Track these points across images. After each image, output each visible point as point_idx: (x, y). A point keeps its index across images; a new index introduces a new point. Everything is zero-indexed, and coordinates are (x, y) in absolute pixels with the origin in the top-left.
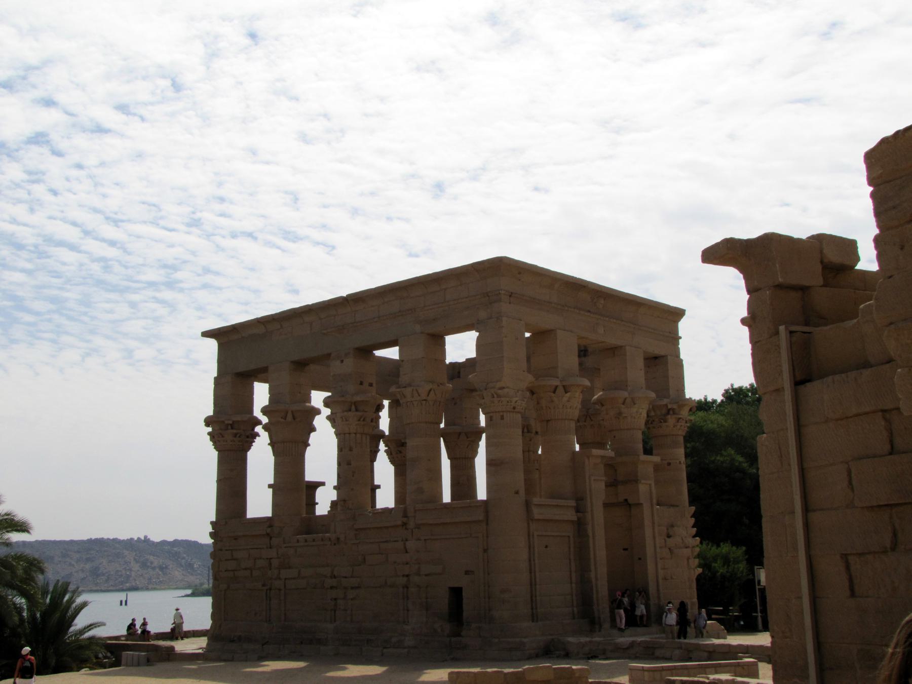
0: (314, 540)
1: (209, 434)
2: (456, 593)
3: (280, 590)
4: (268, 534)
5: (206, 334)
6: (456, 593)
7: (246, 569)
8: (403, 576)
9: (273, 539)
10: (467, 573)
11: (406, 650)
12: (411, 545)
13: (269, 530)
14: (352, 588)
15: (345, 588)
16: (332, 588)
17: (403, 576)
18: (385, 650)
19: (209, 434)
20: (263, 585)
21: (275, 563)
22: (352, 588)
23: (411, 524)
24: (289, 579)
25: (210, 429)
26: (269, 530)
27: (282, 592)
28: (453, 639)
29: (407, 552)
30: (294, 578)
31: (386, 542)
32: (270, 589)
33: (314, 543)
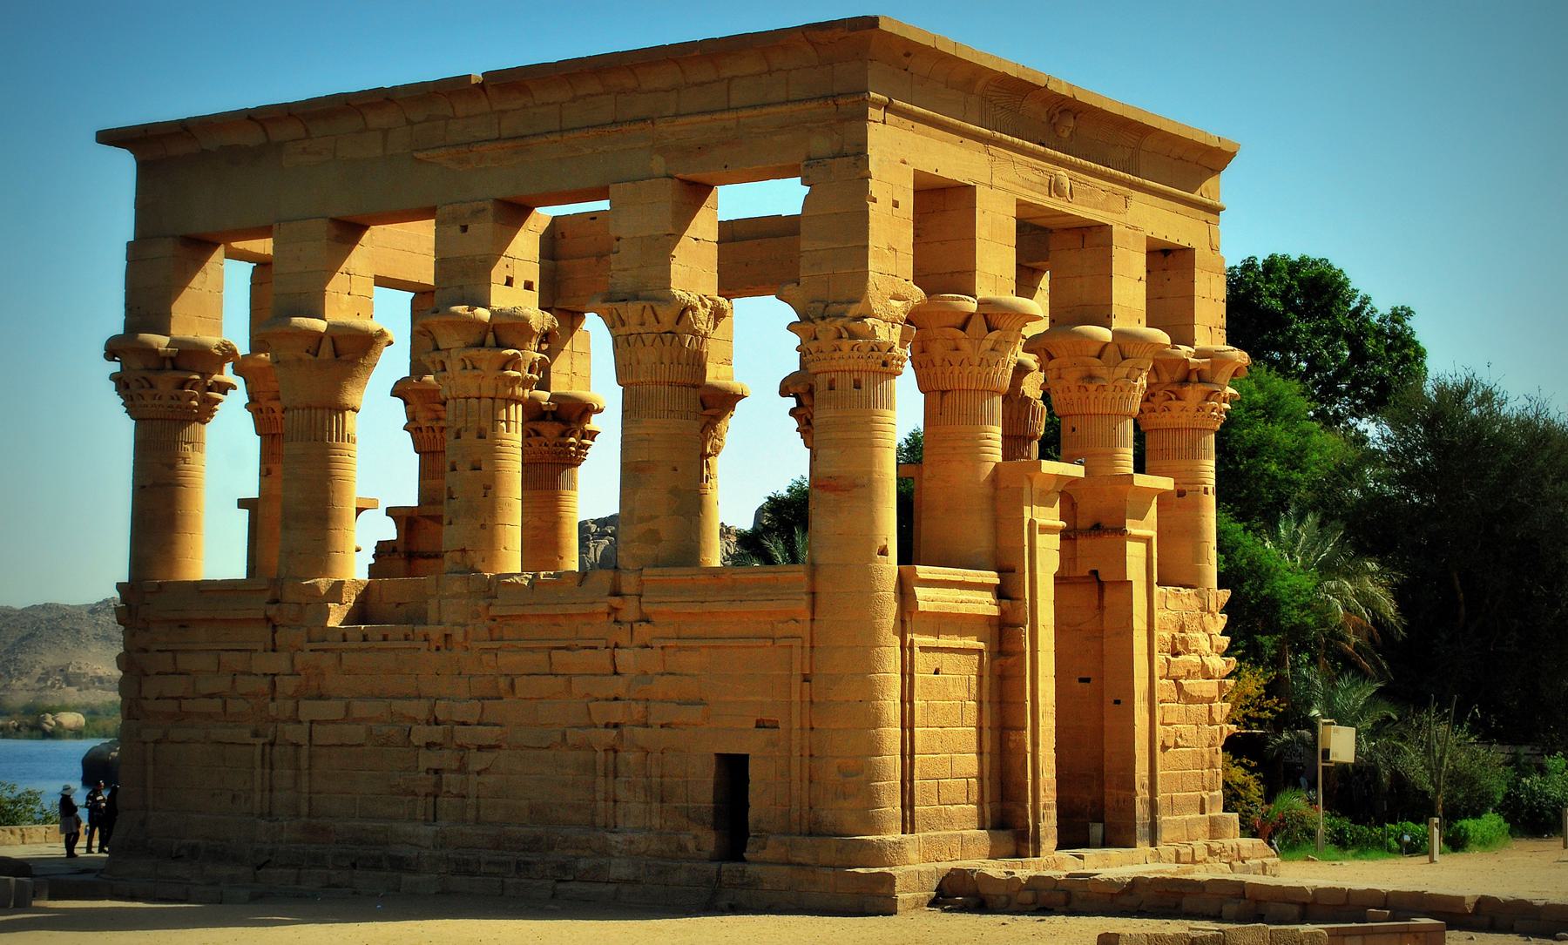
0: (385, 638)
1: (113, 377)
2: (734, 769)
3: (297, 746)
4: (268, 619)
5: (110, 138)
6: (734, 769)
7: (211, 696)
8: (607, 726)
9: (280, 630)
10: (760, 725)
11: (612, 887)
12: (623, 656)
13: (272, 611)
14: (480, 748)
15: (462, 747)
16: (429, 745)
17: (607, 726)
18: (561, 886)
19: (113, 377)
20: (256, 734)
21: (287, 685)
22: (480, 748)
23: (629, 610)
24: (319, 722)
25: (115, 367)
26: (272, 611)
27: (304, 751)
28: (725, 866)
29: (616, 673)
30: (334, 722)
31: (567, 648)
32: (272, 744)
33: (384, 645)
